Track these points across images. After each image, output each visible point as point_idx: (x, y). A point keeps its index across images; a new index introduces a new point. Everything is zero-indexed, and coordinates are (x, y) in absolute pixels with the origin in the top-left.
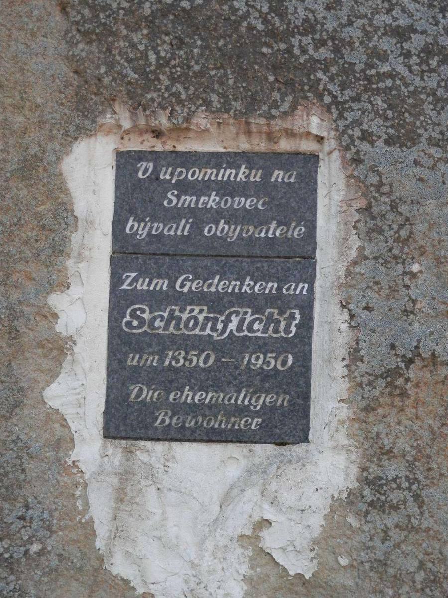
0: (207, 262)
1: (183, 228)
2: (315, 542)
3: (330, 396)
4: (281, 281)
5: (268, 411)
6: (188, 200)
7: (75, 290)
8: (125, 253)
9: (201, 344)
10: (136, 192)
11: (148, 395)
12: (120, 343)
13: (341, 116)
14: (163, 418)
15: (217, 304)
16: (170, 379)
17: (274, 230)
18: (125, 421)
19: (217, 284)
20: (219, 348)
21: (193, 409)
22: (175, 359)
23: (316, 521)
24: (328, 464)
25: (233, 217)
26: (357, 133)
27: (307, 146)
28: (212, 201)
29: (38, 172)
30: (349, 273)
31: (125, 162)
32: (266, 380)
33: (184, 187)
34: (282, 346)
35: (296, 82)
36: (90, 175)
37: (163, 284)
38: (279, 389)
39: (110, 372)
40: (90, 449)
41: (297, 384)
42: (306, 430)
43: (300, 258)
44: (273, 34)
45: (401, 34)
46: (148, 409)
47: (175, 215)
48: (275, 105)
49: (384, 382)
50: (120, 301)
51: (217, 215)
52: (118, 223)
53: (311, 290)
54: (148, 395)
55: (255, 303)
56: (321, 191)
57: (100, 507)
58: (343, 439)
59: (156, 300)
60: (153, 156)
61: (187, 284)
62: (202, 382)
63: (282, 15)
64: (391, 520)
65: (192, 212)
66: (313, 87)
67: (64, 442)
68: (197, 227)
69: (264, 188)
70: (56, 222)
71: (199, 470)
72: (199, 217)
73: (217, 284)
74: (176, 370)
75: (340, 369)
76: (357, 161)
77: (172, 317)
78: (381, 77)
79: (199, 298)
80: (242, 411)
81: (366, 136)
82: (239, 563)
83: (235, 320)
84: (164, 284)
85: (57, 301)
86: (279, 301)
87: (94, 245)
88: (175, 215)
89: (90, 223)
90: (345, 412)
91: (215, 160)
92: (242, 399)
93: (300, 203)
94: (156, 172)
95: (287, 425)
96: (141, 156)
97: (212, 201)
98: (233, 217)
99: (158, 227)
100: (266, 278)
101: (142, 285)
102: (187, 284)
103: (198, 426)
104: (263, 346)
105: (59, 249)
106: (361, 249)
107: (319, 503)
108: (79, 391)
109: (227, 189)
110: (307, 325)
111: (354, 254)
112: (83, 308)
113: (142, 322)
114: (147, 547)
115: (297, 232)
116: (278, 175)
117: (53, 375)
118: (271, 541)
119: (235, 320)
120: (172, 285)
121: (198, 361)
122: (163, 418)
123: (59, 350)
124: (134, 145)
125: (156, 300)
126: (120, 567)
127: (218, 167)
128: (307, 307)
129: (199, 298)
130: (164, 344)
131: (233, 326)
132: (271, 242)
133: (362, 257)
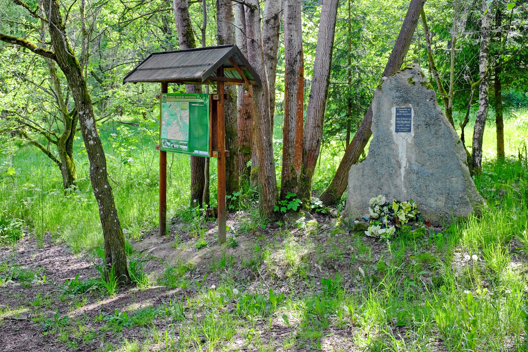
8: (397, 116)
10: (397, 111)
12: (396, 124)
15: (404, 120)
16: (400, 127)
18: (397, 131)
24: (412, 133)
31: (396, 108)
35: (409, 101)
36: (394, 110)
40: (394, 133)
43: (410, 116)
45: (418, 97)
50: (396, 120)
55: (407, 120)
57: (395, 138)
59: (399, 120)
70: (391, 114)
72: (402, 113)
82: (405, 142)
93: (410, 112)
95: (409, 131)
108: (393, 128)
109: (405, 111)
112: (393, 121)
123: (391, 124)
125: (399, 120)
130: (400, 124)
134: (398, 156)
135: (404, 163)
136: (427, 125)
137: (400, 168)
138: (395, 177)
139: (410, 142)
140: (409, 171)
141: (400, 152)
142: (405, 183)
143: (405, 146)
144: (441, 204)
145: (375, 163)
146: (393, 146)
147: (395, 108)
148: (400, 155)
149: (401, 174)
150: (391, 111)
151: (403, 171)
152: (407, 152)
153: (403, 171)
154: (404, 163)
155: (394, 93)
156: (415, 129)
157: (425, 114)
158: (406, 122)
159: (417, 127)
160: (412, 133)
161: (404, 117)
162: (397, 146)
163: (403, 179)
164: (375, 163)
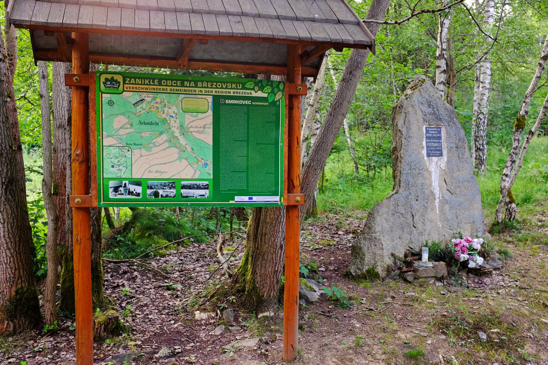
3: (445, 152)
8: (427, 138)
12: (427, 147)
15: (434, 142)
16: (431, 150)
18: (428, 155)
22: (431, 148)
24: (445, 158)
29: (420, 129)
31: (426, 128)
32: (439, 150)
40: (426, 158)
43: (440, 138)
46: (430, 154)
49: (450, 150)
50: (427, 142)
57: (427, 164)
61: (432, 141)
62: (435, 151)
69: (437, 131)
71: (435, 159)
72: (432, 134)
86: (439, 142)
91: (433, 128)
95: (441, 155)
102: (432, 141)
107: (445, 162)
108: (424, 152)
109: (435, 131)
114: (432, 167)
118: (441, 166)
121: (434, 149)
130: (431, 147)
134: (431, 185)
135: (437, 192)
137: (435, 199)
138: (429, 210)
140: (444, 201)
141: (433, 180)
142: (440, 216)
151: (437, 201)
152: (439, 180)
153: (437, 201)
155: (425, 108)
156: (448, 153)
158: (436, 145)
160: (445, 158)
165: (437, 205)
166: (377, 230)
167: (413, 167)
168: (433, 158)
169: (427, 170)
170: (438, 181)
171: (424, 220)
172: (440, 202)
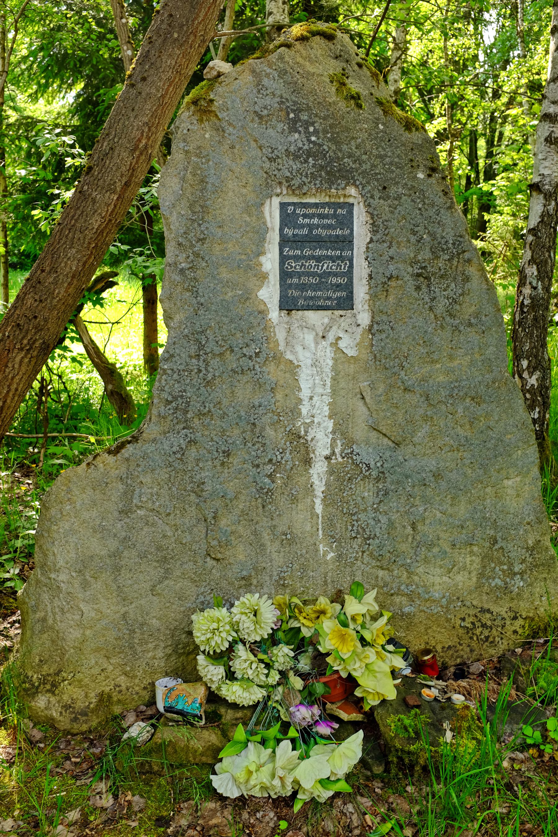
0: (314, 244)
1: (305, 231)
2: (358, 344)
3: (361, 291)
4: (342, 250)
5: (338, 299)
6: (307, 221)
7: (269, 255)
8: (284, 242)
9: (314, 274)
10: (287, 218)
11: (296, 293)
12: (284, 275)
13: (363, 189)
14: (301, 302)
15: (319, 259)
16: (303, 287)
17: (339, 232)
19: (318, 252)
20: (320, 276)
21: (311, 298)
22: (304, 280)
23: (358, 337)
25: (324, 227)
26: (369, 195)
27: (351, 200)
28: (316, 221)
30: (367, 248)
31: (283, 206)
32: (338, 286)
33: (305, 216)
34: (342, 275)
37: (299, 252)
38: (342, 290)
39: (281, 286)
40: (274, 314)
41: (349, 288)
42: (353, 305)
43: (347, 242)
44: (338, 158)
45: (382, 157)
46: (295, 300)
47: (302, 226)
48: (339, 185)
50: (283, 259)
51: (317, 226)
52: (281, 230)
53: (352, 254)
54: (296, 293)
55: (332, 259)
56: (355, 217)
57: (281, 335)
58: (366, 307)
59: (296, 258)
60: (294, 204)
61: (307, 252)
63: (340, 151)
64: (384, 336)
65: (308, 225)
66: (353, 178)
67: (263, 313)
68: (310, 231)
69: (335, 216)
72: (311, 227)
73: (318, 252)
74: (305, 284)
75: (365, 282)
76: (369, 205)
77: (302, 264)
78: (376, 174)
79: (313, 257)
80: (329, 298)
81: (372, 197)
83: (326, 265)
84: (299, 252)
85: (263, 259)
86: (340, 258)
87: (274, 237)
88: (302, 226)
89: (273, 230)
90: (367, 297)
91: (316, 205)
92: (330, 293)
93: (347, 221)
94: (295, 210)
95: (346, 303)
96: (289, 204)
97: (316, 221)
98: (324, 227)
99: (296, 231)
100: (336, 249)
101: (291, 253)
102: (307, 252)
103: (314, 305)
104: (336, 275)
105: (262, 240)
106: (371, 239)
108: (269, 294)
109: (321, 216)
110: (351, 266)
111: (368, 240)
112: (270, 262)
113: (292, 267)
114: (299, 349)
115: (347, 232)
116: (339, 211)
117: (261, 287)
118: (342, 344)
119: (326, 265)
120: (302, 253)
122: (301, 302)
123: (264, 277)
124: (287, 200)
125: (296, 258)
126: (289, 356)
127: (317, 208)
128: (351, 260)
129: (313, 257)
130: (300, 275)
131: (325, 268)
132: (337, 236)
133: (371, 241)
134: (295, 412)
135: (322, 439)
136: (423, 276)
137: (308, 462)
138: (282, 501)
139: (351, 353)
140: (346, 473)
141: (305, 393)
142: (330, 523)
143: (327, 370)
144: (464, 581)
145: (193, 453)
146: (273, 372)
147: (276, 201)
148: (304, 411)
149: (310, 489)
150: (260, 216)
151: (318, 472)
152: (334, 393)
153: (318, 472)
154: (322, 439)
155: (276, 135)
156: (373, 297)
157: (414, 233)
158: (326, 266)
159: (380, 285)
161: (319, 242)
162: (293, 369)
163: (319, 508)
164: (193, 453)
165: (319, 487)
166: (61, 563)
167: (211, 346)
168: (310, 314)
169: (277, 358)
170: (327, 399)
171: (255, 533)
172: (331, 472)
